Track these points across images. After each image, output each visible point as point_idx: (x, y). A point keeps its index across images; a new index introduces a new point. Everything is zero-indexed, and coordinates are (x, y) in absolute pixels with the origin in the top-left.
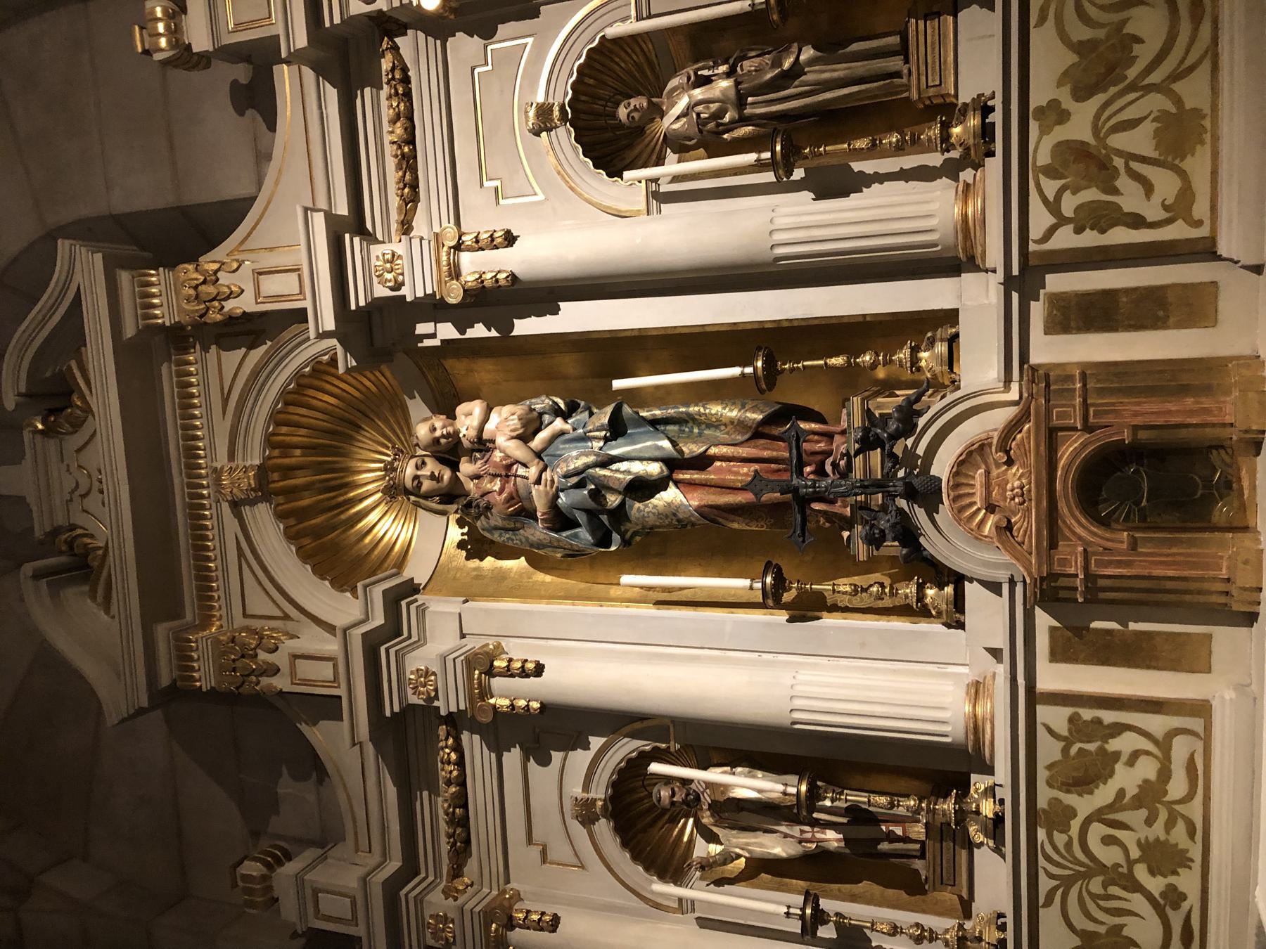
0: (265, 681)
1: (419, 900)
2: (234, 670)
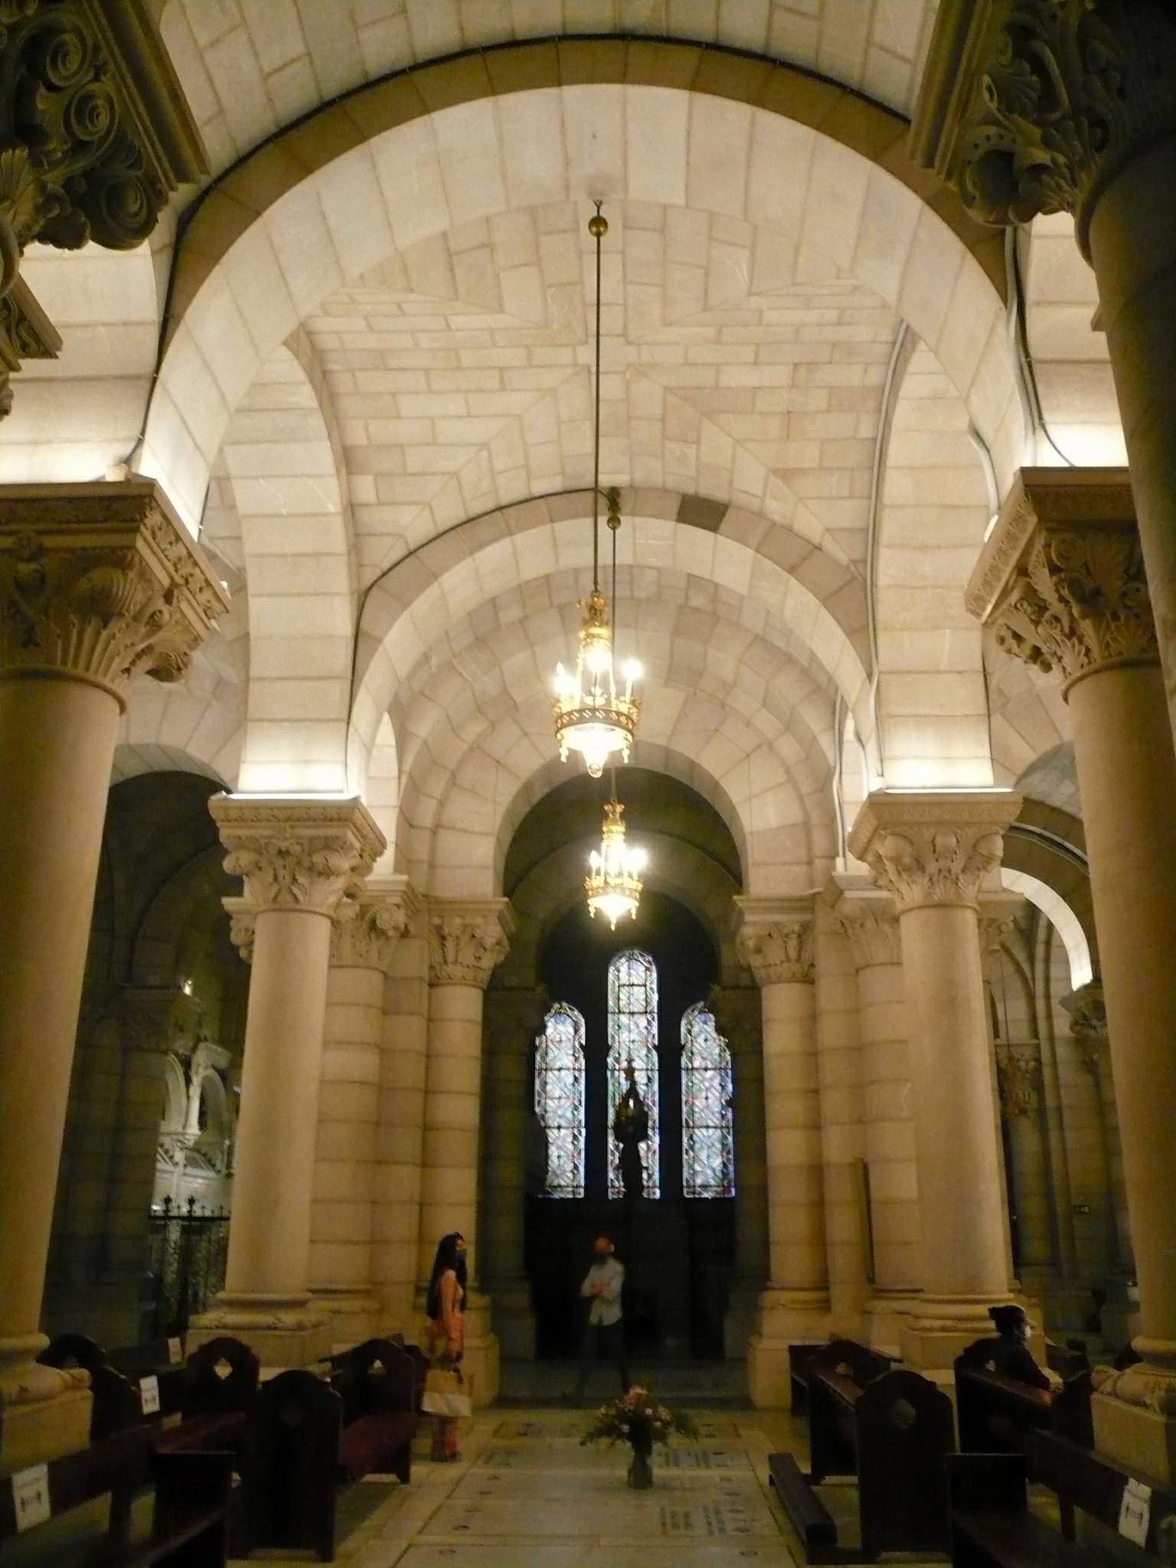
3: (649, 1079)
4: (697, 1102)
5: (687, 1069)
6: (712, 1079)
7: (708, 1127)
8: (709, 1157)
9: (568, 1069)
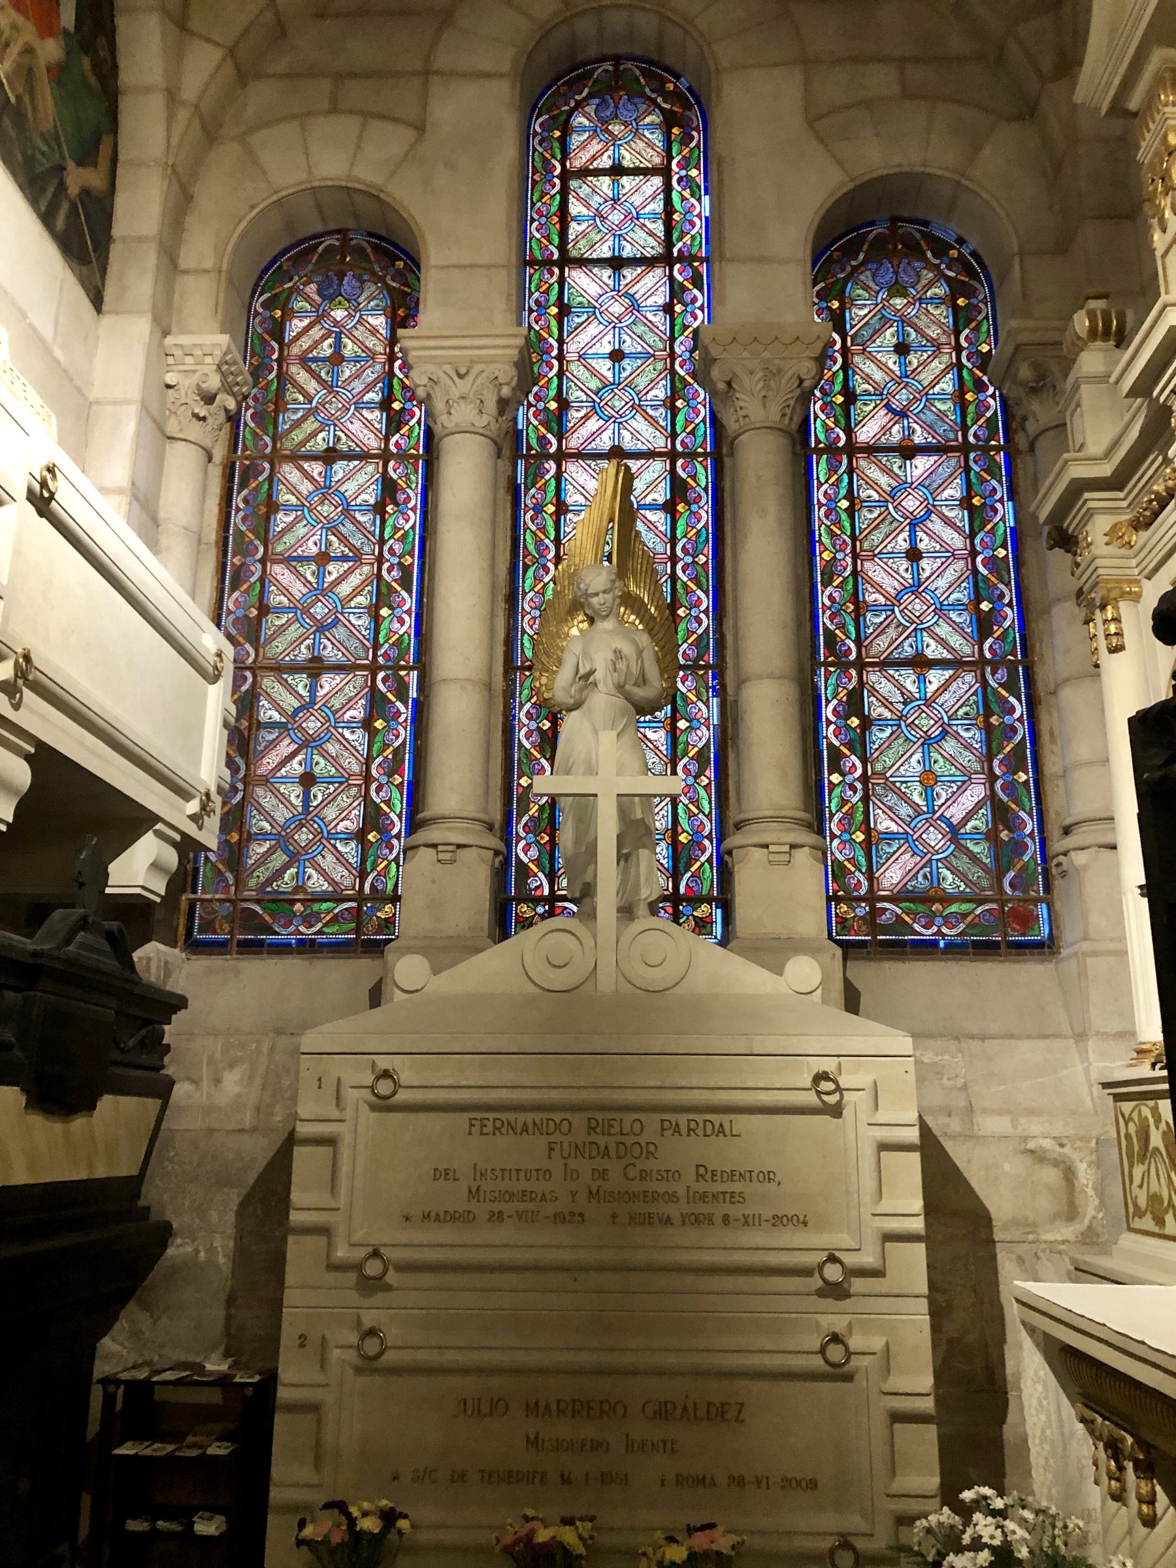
0: (1155, 222)
1: (1091, 514)
2: (1153, 180)
3: (679, 489)
4: (874, 571)
6: (930, 487)
7: (920, 663)
8: (929, 779)
9: (364, 456)
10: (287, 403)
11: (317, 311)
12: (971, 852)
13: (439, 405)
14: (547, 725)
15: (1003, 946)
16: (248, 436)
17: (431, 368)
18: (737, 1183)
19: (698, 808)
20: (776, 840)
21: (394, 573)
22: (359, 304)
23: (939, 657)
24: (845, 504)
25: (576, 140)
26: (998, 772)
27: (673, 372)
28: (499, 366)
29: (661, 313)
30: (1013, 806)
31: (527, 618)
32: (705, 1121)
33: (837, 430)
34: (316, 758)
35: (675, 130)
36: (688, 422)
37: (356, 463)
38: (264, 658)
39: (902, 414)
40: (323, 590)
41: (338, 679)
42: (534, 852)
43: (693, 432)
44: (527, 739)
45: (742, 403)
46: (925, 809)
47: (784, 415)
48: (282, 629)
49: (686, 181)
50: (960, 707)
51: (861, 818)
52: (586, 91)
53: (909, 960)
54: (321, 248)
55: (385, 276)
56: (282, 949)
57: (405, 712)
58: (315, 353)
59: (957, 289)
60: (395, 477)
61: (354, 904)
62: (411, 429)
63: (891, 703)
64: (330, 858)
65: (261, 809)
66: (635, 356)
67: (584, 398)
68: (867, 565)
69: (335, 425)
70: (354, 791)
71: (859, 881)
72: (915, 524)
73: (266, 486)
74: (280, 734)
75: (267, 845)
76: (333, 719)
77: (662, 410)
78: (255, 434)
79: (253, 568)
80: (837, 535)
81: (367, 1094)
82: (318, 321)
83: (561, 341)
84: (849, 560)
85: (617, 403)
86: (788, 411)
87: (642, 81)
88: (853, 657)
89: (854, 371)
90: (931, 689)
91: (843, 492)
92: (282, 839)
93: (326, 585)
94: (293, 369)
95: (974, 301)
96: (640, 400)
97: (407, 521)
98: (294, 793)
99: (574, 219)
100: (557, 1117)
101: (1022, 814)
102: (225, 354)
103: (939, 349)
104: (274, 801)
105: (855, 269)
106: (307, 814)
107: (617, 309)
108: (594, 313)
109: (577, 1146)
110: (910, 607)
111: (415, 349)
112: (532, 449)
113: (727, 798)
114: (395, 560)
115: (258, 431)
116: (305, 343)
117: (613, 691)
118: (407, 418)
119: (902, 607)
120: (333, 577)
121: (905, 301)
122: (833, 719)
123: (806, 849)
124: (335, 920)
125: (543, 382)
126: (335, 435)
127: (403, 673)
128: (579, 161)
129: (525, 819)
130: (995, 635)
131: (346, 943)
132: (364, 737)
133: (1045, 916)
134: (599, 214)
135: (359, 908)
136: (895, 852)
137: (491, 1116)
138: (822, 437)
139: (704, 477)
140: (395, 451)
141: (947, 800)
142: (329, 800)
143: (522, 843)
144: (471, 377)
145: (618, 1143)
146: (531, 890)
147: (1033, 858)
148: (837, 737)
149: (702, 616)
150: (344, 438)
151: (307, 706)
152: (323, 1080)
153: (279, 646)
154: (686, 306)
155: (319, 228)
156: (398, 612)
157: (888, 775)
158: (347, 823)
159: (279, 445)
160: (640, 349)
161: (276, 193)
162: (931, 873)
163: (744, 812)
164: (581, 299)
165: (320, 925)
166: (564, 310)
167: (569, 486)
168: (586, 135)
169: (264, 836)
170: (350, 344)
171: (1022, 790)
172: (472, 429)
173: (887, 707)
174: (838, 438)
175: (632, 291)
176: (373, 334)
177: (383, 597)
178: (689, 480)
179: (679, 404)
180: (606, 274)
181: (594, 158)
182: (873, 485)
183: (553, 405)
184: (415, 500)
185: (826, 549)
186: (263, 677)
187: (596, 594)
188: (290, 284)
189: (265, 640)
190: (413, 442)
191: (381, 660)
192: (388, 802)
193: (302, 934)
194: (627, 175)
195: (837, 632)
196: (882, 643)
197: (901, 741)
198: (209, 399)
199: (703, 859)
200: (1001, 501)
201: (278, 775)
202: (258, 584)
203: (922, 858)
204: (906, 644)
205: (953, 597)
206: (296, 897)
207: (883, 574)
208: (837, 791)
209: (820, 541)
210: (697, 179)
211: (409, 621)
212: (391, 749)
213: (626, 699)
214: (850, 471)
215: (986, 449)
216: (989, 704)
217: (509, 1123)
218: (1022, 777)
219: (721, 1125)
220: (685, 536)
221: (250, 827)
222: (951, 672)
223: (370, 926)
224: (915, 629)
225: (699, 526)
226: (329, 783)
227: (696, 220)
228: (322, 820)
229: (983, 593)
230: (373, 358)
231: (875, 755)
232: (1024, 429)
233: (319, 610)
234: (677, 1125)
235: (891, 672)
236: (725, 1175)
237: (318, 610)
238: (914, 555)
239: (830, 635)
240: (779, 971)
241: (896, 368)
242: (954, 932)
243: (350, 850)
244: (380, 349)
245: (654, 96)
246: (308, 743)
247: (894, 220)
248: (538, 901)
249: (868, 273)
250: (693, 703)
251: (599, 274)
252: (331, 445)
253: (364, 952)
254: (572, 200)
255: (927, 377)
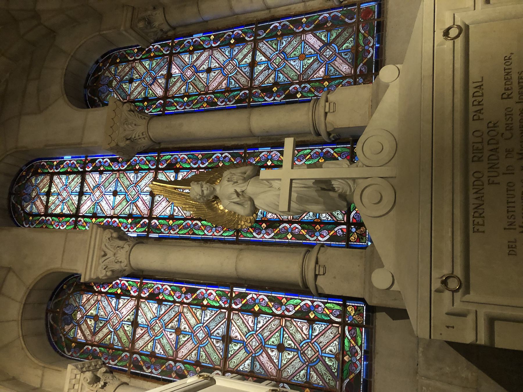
4: (213, 86)
5: (164, 106)
7: (253, 64)
8: (302, 57)
9: (137, 308)
10: (110, 343)
11: (76, 326)
12: (336, 37)
13: (117, 267)
14: (264, 225)
15: (379, 20)
16: (121, 364)
17: (100, 268)
18: (513, 76)
19: (308, 155)
20: (323, 108)
21: (189, 297)
22: (77, 306)
23: (251, 57)
24: (186, 99)
25: (35, 210)
26: (302, 30)
27: (126, 170)
28: (104, 237)
29: (102, 175)
30: (317, 22)
31: (215, 234)
32: (473, 97)
33: (157, 104)
34: (270, 342)
35: (39, 171)
36: (145, 164)
37: (139, 312)
38: (220, 366)
39: (155, 79)
40: (192, 332)
41: (233, 328)
42: (325, 233)
43: (149, 162)
44: (270, 234)
45: (137, 135)
46: (315, 57)
47: (144, 118)
48: (208, 355)
49: (58, 166)
50: (272, 47)
51: (317, 83)
52: (19, 206)
53: (385, 57)
54: (52, 323)
55: (68, 293)
56: (369, 369)
57: (252, 295)
58: (92, 328)
59: (114, 63)
60: (148, 294)
61: (346, 328)
62: (130, 285)
63: (268, 75)
64: (321, 339)
65: (294, 375)
66: (117, 186)
67: (129, 207)
68: (211, 88)
69: (123, 321)
70: (288, 324)
71: (346, 82)
72: (197, 71)
73: (143, 357)
74: (257, 361)
75: (312, 373)
76: (252, 332)
77: (139, 175)
78: (120, 361)
79: (178, 367)
80: (197, 101)
81: (458, 295)
82: (80, 326)
83: (106, 217)
84: (207, 96)
85: (133, 193)
86: (143, 117)
87: (20, 184)
88: (247, 92)
89: (136, 99)
90: (264, 59)
91: (181, 100)
92: (310, 364)
93: (190, 331)
94: (97, 339)
95: (119, 56)
96: (133, 184)
97: (167, 289)
98: (287, 356)
99: (62, 211)
100: (472, 179)
101: (320, 19)
102: (77, 368)
103: (133, 67)
104: (290, 367)
105: (100, 101)
106: (299, 351)
107: (98, 194)
108: (98, 203)
109: (491, 168)
110: (229, 70)
111: (90, 275)
112: (145, 230)
113: (304, 141)
114: (183, 296)
115: (119, 358)
116: (87, 333)
117: (247, 183)
118: (125, 287)
119: (229, 73)
120: (187, 327)
121: (114, 81)
122: (273, 98)
123: (328, 96)
124: (354, 338)
125: (120, 225)
126: (126, 321)
127: (234, 295)
128: (42, 209)
129: (308, 236)
130: (244, 36)
131: (367, 333)
132: (262, 317)
133: (366, 4)
134: (62, 201)
135: (349, 325)
136: (334, 68)
137: (471, 219)
138: (159, 109)
139: (167, 156)
140: (137, 293)
141: (312, 49)
142: (292, 337)
143: (320, 238)
144: (107, 250)
145: (488, 144)
146: (343, 234)
147: (340, 12)
148: (281, 96)
149: (223, 156)
150: (129, 317)
151: (245, 346)
152: (448, 325)
153: (215, 357)
154: (101, 165)
155: (43, 322)
156: (206, 296)
157: (299, 73)
158: (304, 328)
159: (127, 349)
160: (114, 184)
161: (19, 337)
162: (344, 53)
163: (310, 131)
164: (91, 208)
165: (356, 347)
166: (95, 216)
167: (163, 214)
168: (34, 206)
169: (308, 374)
170: (92, 311)
171: (309, 20)
172: (128, 252)
173: (270, 76)
174: (160, 103)
175: (92, 187)
176: (89, 300)
177: (198, 303)
178: (167, 163)
179: (137, 167)
180: (84, 198)
181: (42, 203)
182: (180, 88)
183: (130, 221)
184: (159, 285)
185: (202, 105)
186: (229, 367)
187: (202, 191)
188: (63, 338)
189: (212, 364)
190: (135, 284)
191: (227, 306)
192: (295, 306)
193: (361, 357)
194: (51, 190)
195: (236, 99)
196: (243, 80)
197: (285, 70)
198: (96, 379)
199: (332, 152)
200: (192, 39)
201: (277, 363)
202: (186, 365)
203: (337, 56)
204: (244, 70)
205: (227, 54)
206: (341, 359)
207: (215, 82)
208: (304, 94)
209: (199, 108)
210: (57, 162)
211: (211, 290)
212: (269, 303)
213: (251, 178)
214: (173, 97)
215: (172, 47)
216: (274, 36)
217: (476, 208)
218: (304, 20)
219: (476, 87)
220: (190, 164)
221: (303, 381)
222: (258, 52)
223: (358, 319)
224: (239, 67)
225: (186, 157)
226: (283, 337)
227: (72, 162)
228: (302, 342)
229: (227, 42)
230: (99, 301)
231: (290, 79)
232: (166, 33)
233: (201, 335)
234: (476, 111)
235: (255, 76)
236: (509, 83)
237: (201, 336)
238: (209, 70)
239: (237, 102)
240: (387, 86)
241: (138, 83)
242: (372, 41)
243: (318, 327)
244: (95, 298)
245: (26, 179)
246: (263, 346)
247: (86, 87)
248: (349, 231)
249: (102, 95)
250: (260, 158)
251: (84, 201)
252: (130, 323)
253: (372, 324)
254: (55, 212)
255: (142, 71)
